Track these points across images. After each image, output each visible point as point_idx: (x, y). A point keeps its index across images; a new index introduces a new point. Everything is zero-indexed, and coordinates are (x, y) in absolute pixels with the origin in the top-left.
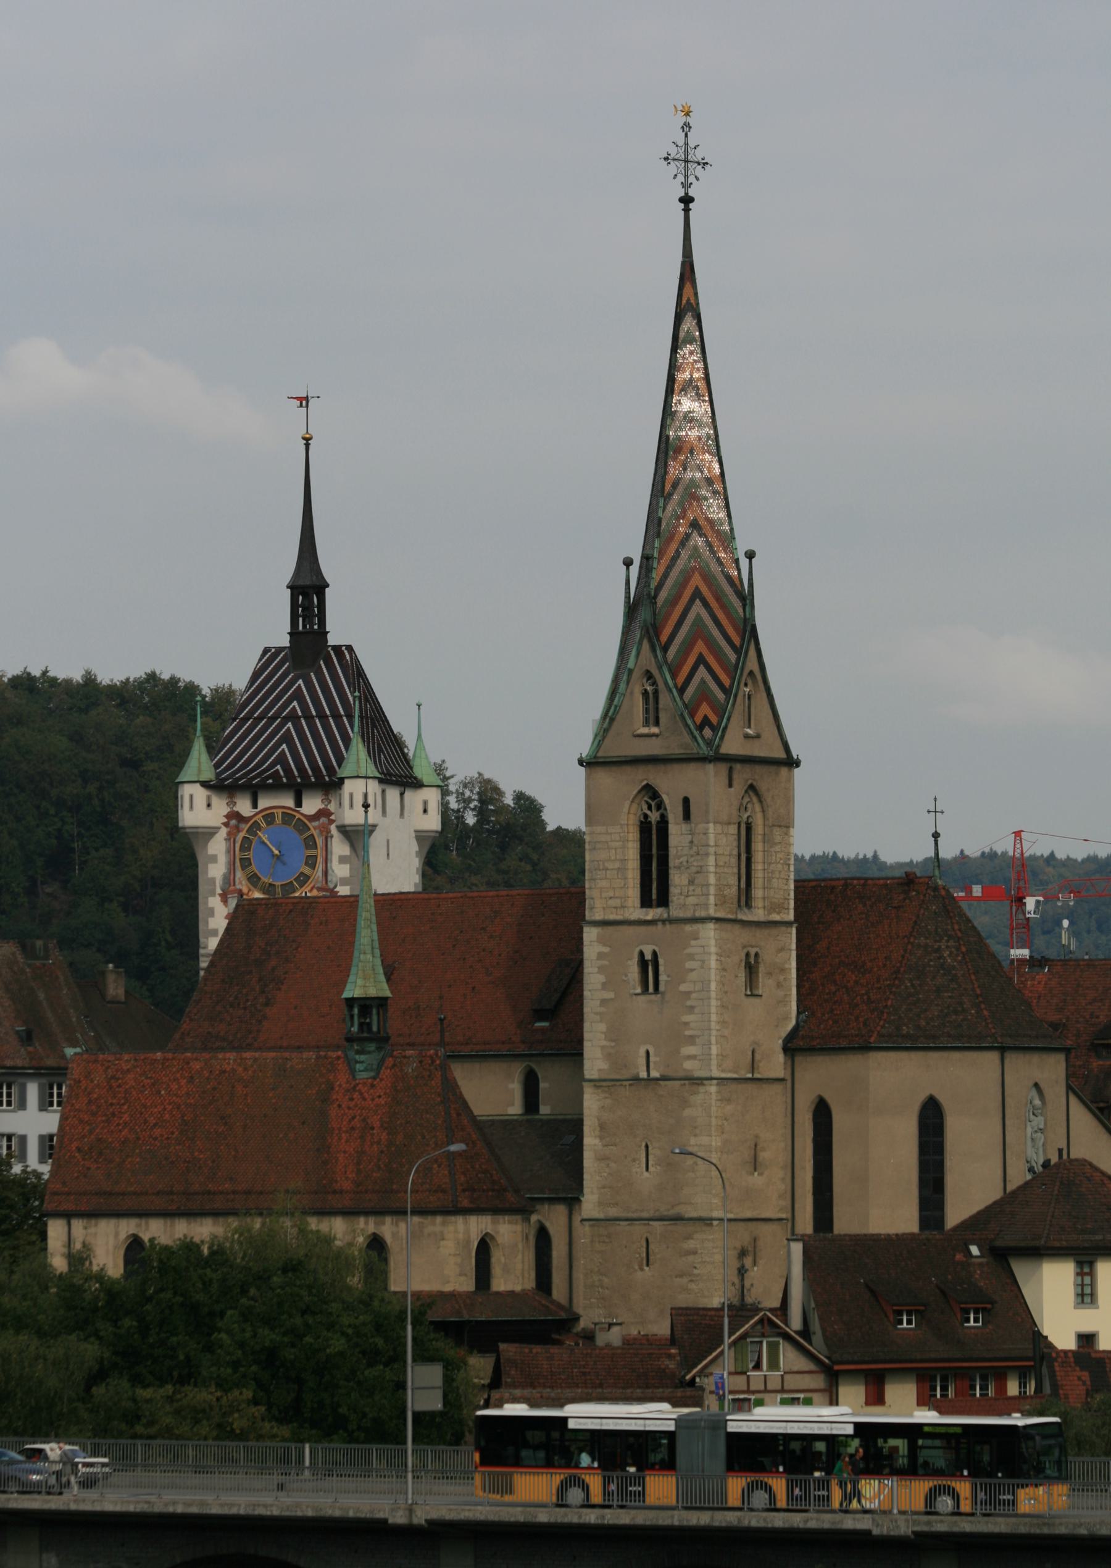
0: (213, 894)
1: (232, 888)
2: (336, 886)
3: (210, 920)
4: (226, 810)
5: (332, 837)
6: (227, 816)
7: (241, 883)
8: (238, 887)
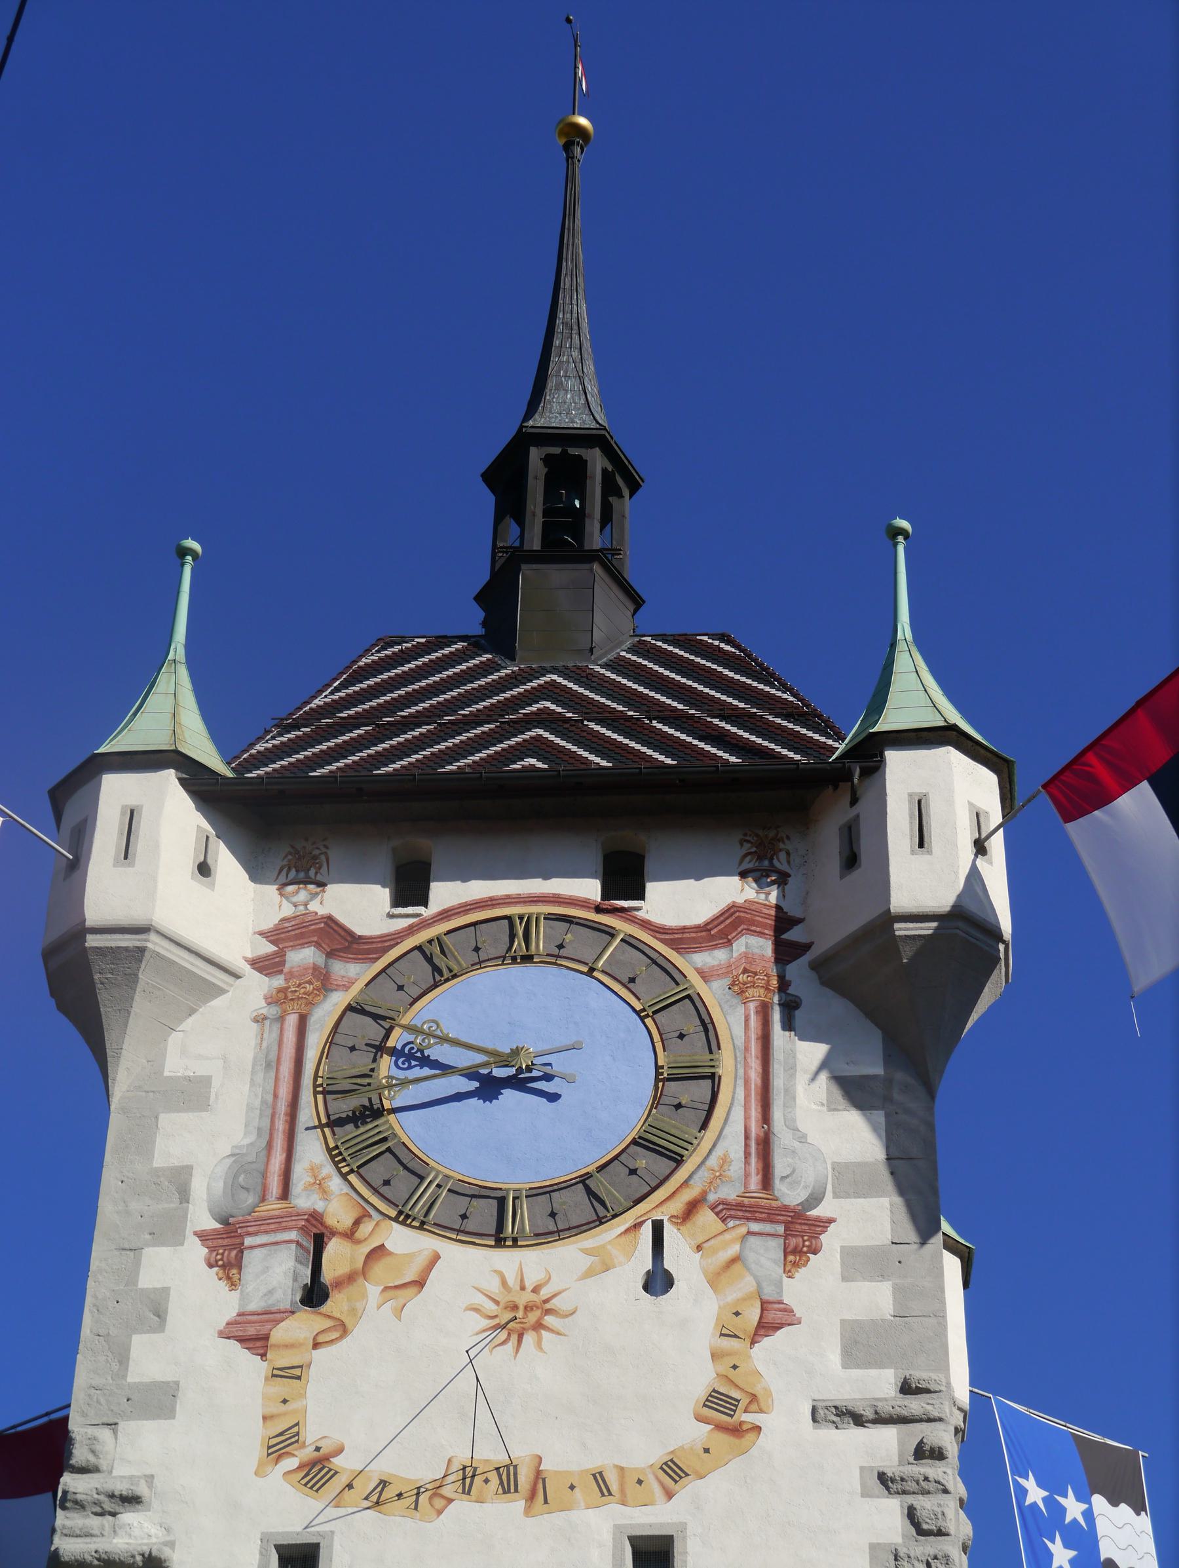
0: (168, 1231)
1: (273, 1206)
2: (815, 1199)
3: (140, 1344)
7: (320, 1185)
8: (304, 1200)
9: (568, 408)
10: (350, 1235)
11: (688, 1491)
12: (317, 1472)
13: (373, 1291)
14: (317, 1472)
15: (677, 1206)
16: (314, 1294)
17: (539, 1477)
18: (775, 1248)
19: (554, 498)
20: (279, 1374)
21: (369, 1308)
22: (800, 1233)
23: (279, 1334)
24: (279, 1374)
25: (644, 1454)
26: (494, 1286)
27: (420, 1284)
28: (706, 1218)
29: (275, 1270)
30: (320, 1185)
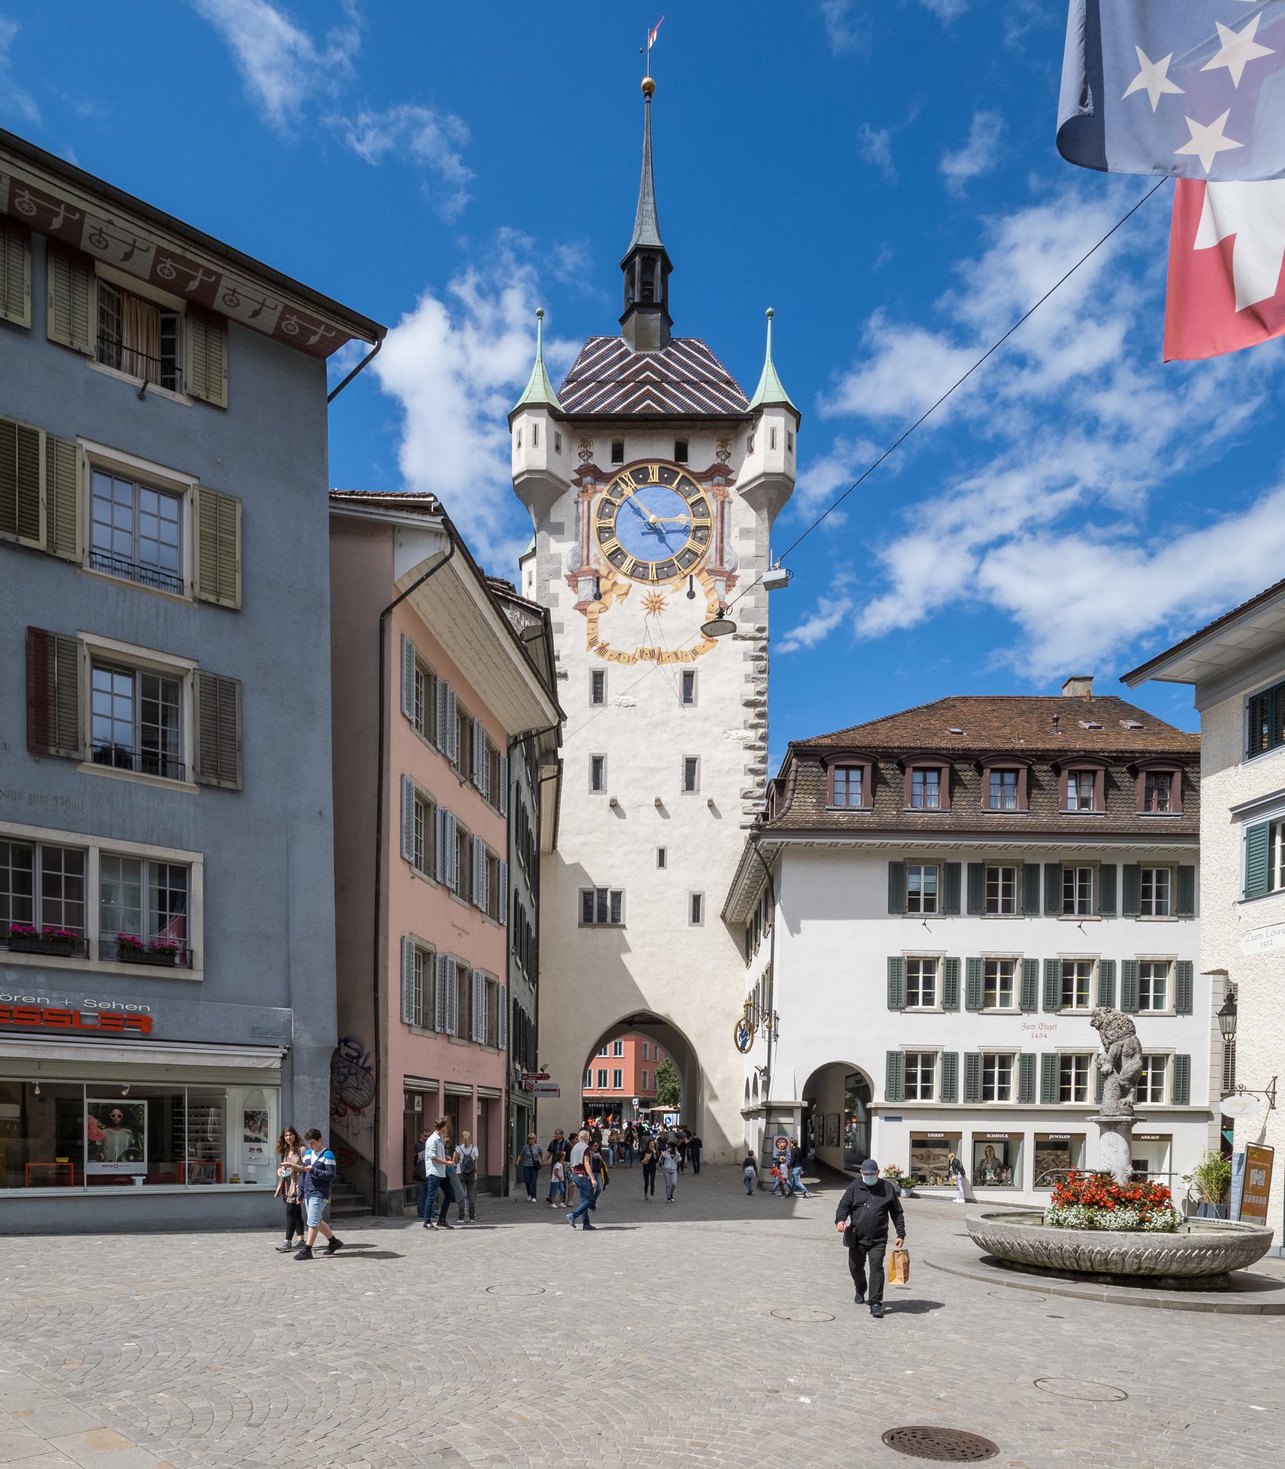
0: (556, 574)
1: (585, 568)
2: (734, 569)
4: (578, 463)
5: (730, 503)
6: (577, 471)
7: (597, 561)
8: (594, 566)
9: (648, 236)
10: (606, 577)
11: (699, 658)
12: (602, 650)
13: (614, 596)
14: (602, 650)
15: (696, 571)
16: (598, 596)
17: (660, 654)
18: (723, 584)
19: (647, 275)
20: (590, 621)
21: (611, 599)
22: (730, 579)
23: (589, 608)
24: (590, 621)
25: (688, 648)
26: (646, 595)
27: (626, 594)
28: (704, 574)
29: (587, 588)
30: (597, 561)
